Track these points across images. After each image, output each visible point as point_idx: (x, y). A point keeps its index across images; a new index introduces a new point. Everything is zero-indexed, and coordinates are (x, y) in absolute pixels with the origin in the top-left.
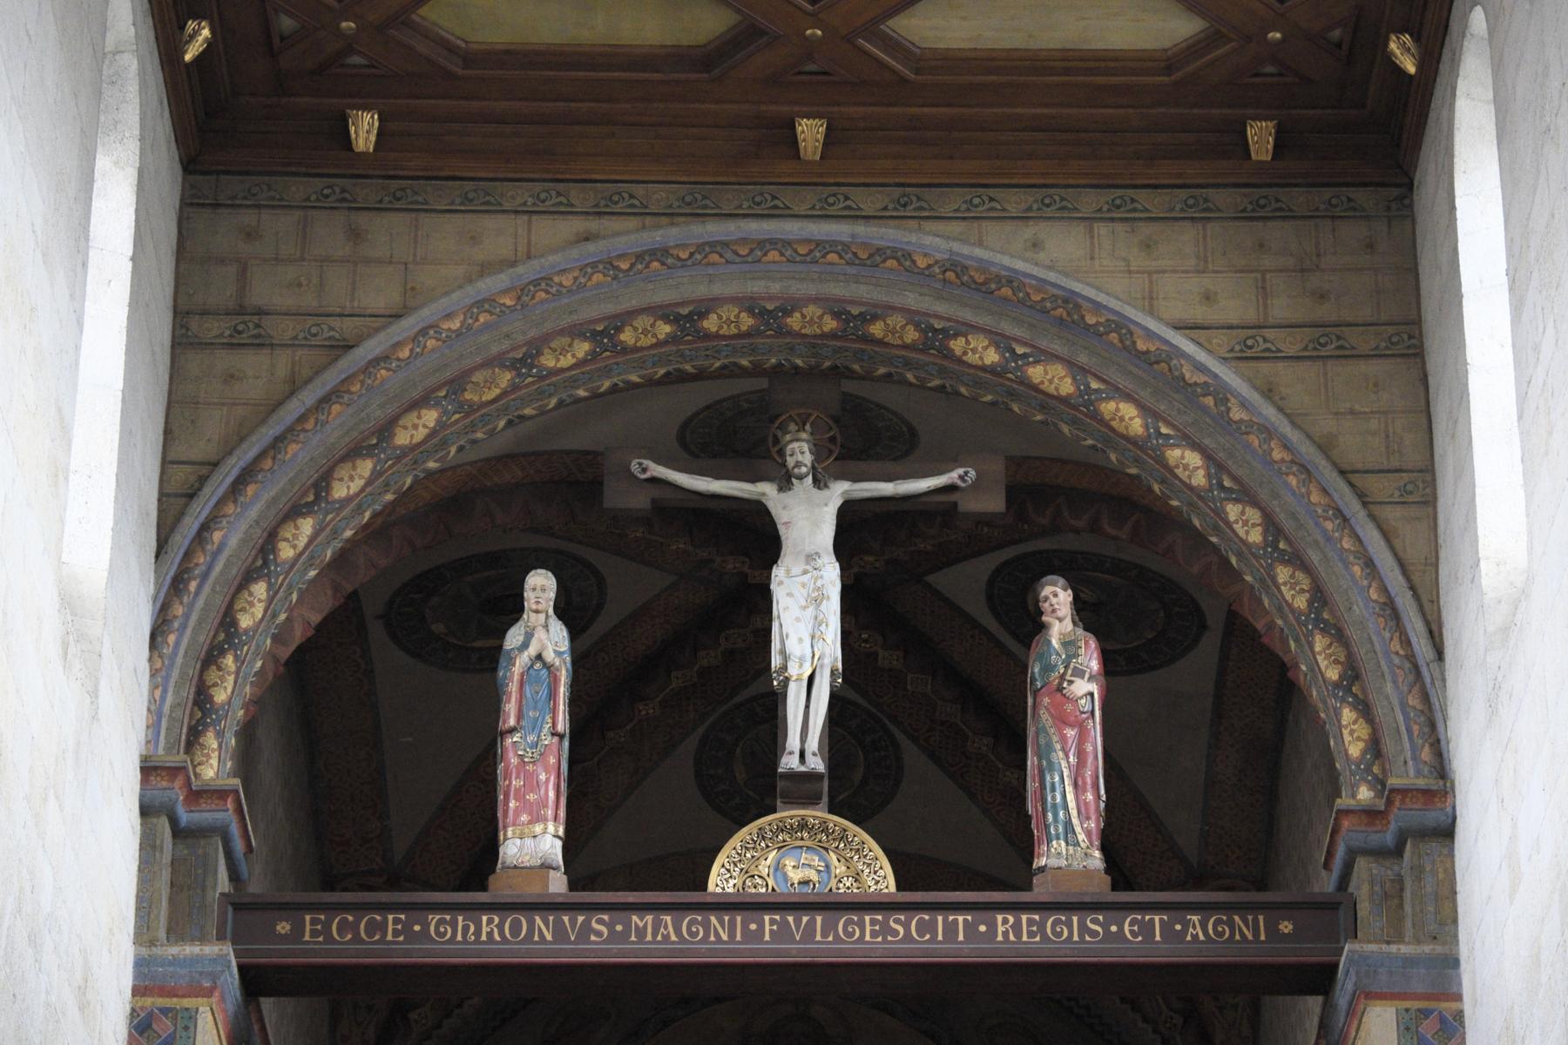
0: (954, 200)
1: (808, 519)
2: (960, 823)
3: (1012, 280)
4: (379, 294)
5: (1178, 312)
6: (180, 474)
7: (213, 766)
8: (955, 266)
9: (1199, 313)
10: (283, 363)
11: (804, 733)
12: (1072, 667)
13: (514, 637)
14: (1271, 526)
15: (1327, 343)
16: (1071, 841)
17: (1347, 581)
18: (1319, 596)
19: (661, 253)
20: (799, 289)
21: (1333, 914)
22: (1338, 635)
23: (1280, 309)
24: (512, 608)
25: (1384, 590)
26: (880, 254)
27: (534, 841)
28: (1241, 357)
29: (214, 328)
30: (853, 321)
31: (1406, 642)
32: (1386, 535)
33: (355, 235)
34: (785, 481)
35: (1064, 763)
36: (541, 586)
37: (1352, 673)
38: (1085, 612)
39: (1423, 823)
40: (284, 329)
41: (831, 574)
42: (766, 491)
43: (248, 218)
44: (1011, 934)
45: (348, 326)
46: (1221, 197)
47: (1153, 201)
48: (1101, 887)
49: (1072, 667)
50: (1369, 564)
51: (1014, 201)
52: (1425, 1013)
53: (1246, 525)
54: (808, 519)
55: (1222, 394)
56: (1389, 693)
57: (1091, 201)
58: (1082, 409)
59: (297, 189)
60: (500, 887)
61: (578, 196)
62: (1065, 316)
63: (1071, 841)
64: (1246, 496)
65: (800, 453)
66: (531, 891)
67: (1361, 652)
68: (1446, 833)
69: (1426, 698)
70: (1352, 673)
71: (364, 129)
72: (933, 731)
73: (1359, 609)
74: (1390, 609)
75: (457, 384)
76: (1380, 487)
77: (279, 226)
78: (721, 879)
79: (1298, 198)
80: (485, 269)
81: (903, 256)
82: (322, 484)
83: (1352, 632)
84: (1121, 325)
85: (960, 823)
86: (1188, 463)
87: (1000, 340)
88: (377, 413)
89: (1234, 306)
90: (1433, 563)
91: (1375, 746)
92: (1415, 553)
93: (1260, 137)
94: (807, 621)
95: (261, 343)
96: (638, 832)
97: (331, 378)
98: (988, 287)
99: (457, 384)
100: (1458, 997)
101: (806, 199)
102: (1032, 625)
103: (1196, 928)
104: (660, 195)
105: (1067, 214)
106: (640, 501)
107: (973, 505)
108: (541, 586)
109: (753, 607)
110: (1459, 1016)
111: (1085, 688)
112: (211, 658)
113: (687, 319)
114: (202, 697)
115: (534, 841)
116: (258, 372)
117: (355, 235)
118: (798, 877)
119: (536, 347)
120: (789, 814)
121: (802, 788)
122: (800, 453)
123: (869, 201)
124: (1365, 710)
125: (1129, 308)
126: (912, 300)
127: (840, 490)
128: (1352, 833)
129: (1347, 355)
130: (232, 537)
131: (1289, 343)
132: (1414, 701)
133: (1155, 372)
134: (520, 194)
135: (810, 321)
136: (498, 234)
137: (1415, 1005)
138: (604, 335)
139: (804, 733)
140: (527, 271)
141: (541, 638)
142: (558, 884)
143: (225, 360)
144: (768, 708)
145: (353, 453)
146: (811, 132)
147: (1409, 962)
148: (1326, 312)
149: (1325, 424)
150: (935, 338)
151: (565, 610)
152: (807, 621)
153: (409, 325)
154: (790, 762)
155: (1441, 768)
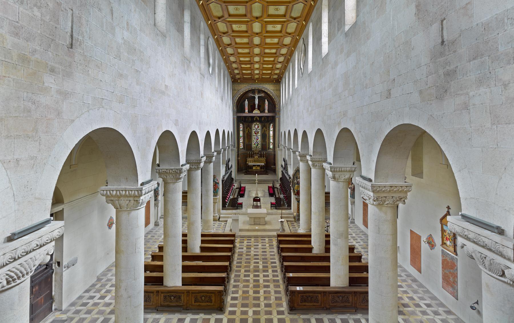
1: (257, 97)
2: (263, 111)
12: (266, 102)
15: (277, 90)
16: (266, 111)
27: (247, 111)
39: (279, 111)
44: (264, 115)
49: (266, 102)
54: (257, 97)
63: (266, 111)
72: (261, 108)
85: (263, 111)
94: (257, 102)
96: (251, 111)
115: (247, 111)
116: (236, 92)
125: (269, 88)
136: (244, 85)
144: (255, 105)
152: (257, 102)
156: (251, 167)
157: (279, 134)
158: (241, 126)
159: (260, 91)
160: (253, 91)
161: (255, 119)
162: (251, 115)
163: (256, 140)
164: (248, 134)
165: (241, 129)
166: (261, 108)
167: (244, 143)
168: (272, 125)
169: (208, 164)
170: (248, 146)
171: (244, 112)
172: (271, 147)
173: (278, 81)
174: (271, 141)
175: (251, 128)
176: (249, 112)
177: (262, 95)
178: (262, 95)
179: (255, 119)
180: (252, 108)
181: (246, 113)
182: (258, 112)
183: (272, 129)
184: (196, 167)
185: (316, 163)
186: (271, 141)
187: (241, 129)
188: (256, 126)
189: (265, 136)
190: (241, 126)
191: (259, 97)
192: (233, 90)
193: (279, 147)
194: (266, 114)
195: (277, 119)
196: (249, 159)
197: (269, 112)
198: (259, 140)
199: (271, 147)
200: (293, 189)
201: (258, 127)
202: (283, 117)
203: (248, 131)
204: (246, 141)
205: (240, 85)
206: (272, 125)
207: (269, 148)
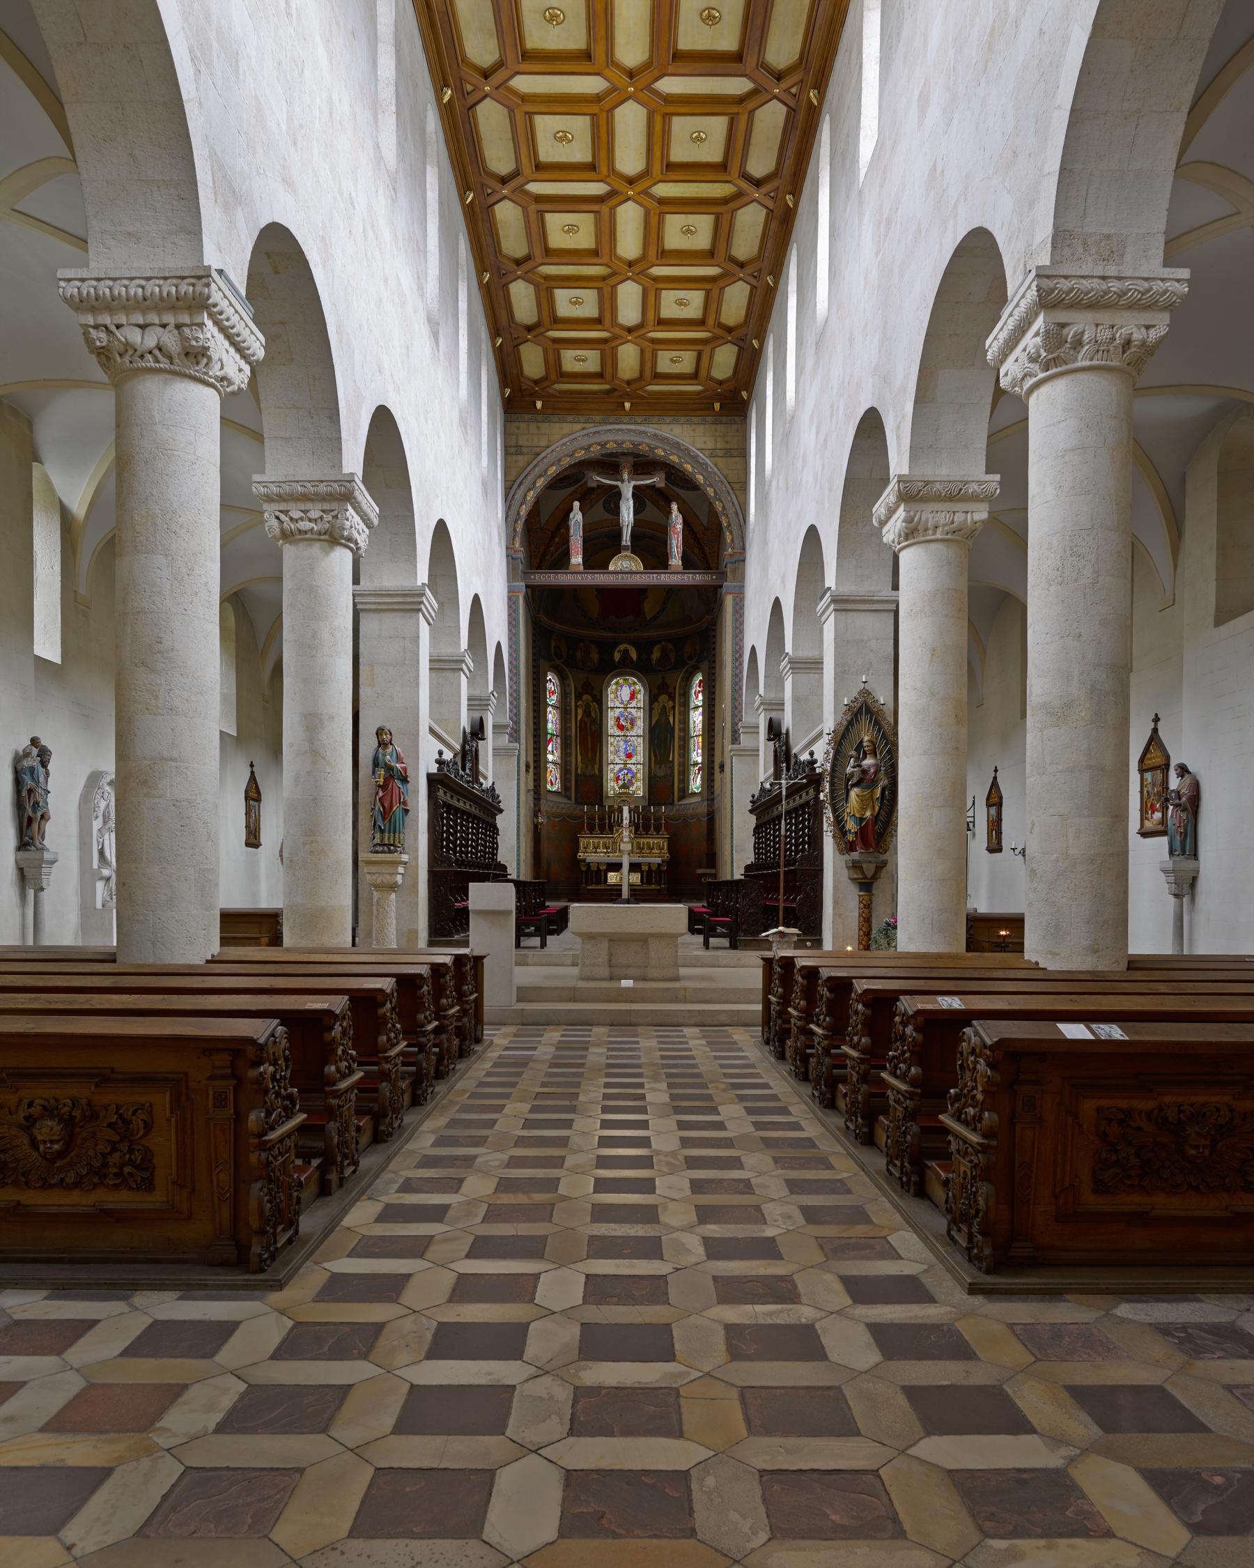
0: (655, 419)
1: (627, 490)
3: (667, 439)
4: (543, 443)
5: (698, 446)
6: (509, 484)
7: (517, 545)
8: (655, 435)
9: (703, 446)
10: (526, 458)
11: (626, 539)
13: (571, 515)
14: (715, 492)
15: (728, 453)
16: (676, 561)
17: (729, 506)
18: (724, 508)
19: (598, 432)
20: (626, 438)
21: (723, 576)
22: (727, 517)
23: (719, 446)
24: (571, 509)
26: (641, 432)
27: (577, 559)
28: (712, 456)
29: (513, 450)
30: (636, 445)
33: (538, 428)
34: (623, 481)
35: (674, 542)
36: (576, 504)
37: (729, 525)
38: (680, 510)
40: (525, 450)
41: (631, 502)
42: (619, 483)
43: (517, 424)
44: (664, 579)
45: (537, 450)
46: (709, 419)
47: (695, 419)
48: (681, 569)
51: (668, 419)
53: (710, 491)
54: (627, 490)
55: (706, 465)
56: (735, 528)
57: (683, 419)
58: (681, 464)
59: (527, 417)
60: (572, 569)
61: (582, 419)
62: (677, 446)
63: (676, 561)
64: (711, 486)
65: (626, 476)
66: (576, 570)
68: (744, 561)
70: (729, 525)
71: (539, 404)
73: (731, 512)
74: (737, 514)
75: (559, 460)
76: (736, 486)
77: (523, 425)
78: (611, 568)
79: (724, 419)
80: (564, 436)
81: (645, 433)
82: (534, 483)
84: (687, 449)
86: (700, 478)
87: (664, 450)
88: (542, 467)
89: (710, 445)
91: (732, 541)
93: (717, 406)
95: (521, 454)
97: (535, 463)
98: (664, 440)
99: (559, 460)
101: (626, 419)
102: (670, 513)
103: (698, 577)
104: (598, 418)
105: (678, 422)
106: (594, 485)
107: (658, 485)
108: (576, 504)
109: (616, 511)
111: (679, 527)
112: (516, 522)
113: (603, 445)
114: (515, 530)
115: (577, 559)
116: (522, 460)
117: (538, 428)
118: (625, 568)
119: (574, 452)
120: (623, 553)
121: (626, 548)
122: (626, 476)
123: (639, 419)
124: (731, 533)
126: (647, 441)
127: (633, 483)
128: (727, 559)
129: (731, 456)
130: (519, 496)
131: (720, 453)
133: (695, 459)
134: (570, 418)
135: (627, 445)
136: (567, 428)
138: (587, 448)
139: (626, 539)
140: (572, 437)
141: (576, 517)
142: (581, 568)
143: (515, 457)
145: (540, 476)
146: (627, 405)
148: (728, 446)
149: (726, 472)
150: (652, 449)
151: (581, 509)
153: (549, 450)
154: (624, 543)
155: (744, 549)
156: (598, 874)
157: (737, 676)
158: (552, 683)
159: (643, 465)
160: (609, 464)
161: (617, 656)
162: (598, 579)
163: (625, 760)
164: (582, 727)
165: (553, 699)
166: (650, 547)
167: (565, 766)
168: (699, 677)
169: (316, 549)
170: (585, 782)
171: (562, 561)
172: (696, 784)
173: (733, 402)
174: (697, 756)
175: (599, 700)
176: (589, 564)
177: (657, 480)
178: (657, 480)
179: (617, 656)
180: (602, 546)
181: (576, 572)
182: (635, 564)
183: (698, 699)
184: (170, 340)
185: (1082, 324)
186: (697, 756)
187: (553, 699)
188: (625, 693)
189: (664, 738)
190: (552, 683)
191: (638, 493)
192: (511, 450)
193: (735, 739)
194: (676, 574)
195: (729, 601)
196: (583, 842)
197: (688, 563)
198: (640, 757)
199: (696, 784)
201: (633, 696)
202: (765, 543)
203: (587, 713)
204: (577, 759)
205: (544, 426)
206: (699, 677)
207: (684, 792)
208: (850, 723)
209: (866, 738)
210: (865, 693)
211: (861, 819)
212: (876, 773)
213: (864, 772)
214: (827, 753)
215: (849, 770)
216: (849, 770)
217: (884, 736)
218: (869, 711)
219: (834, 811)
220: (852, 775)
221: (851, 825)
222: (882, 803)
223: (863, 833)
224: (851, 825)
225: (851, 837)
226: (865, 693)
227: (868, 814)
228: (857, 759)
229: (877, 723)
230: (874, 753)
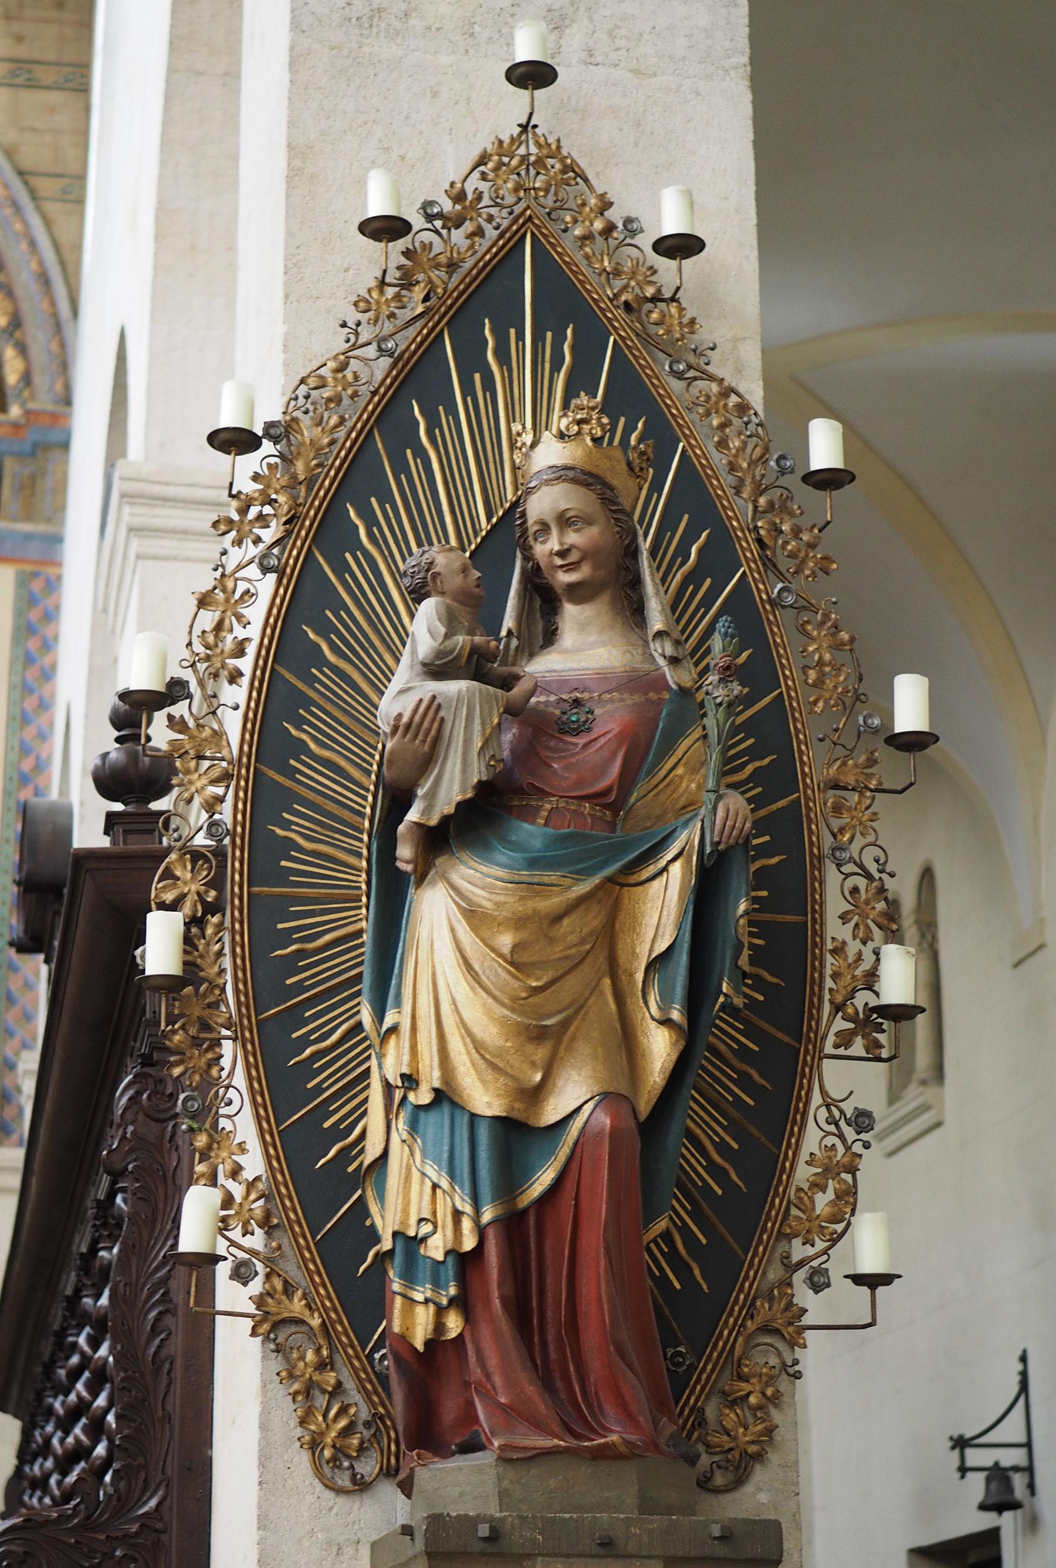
25: (41, 263)
31: (53, 304)
32: (48, 223)
50: (32, 243)
52: (35, 575)
56: (38, 338)
67: (25, 308)
69: (63, 345)
83: (19, 292)
90: (78, 246)
91: (27, 378)
92: (64, 239)
100: (59, 564)
110: (59, 578)
124: (22, 349)
132: (54, 347)
137: (29, 568)
147: (28, 537)
200: (321, 1187)
208: (415, 378)
209: (551, 453)
210: (537, 177)
211: (516, 1136)
212: (643, 749)
213: (542, 727)
214: (220, 597)
215: (401, 694)
216: (401, 694)
217: (693, 496)
218: (564, 302)
219: (282, 1089)
220: (427, 734)
221: (420, 1198)
222: (697, 999)
223: (520, 1259)
224: (420, 1198)
225: (416, 1316)
226: (537, 177)
227: (572, 1094)
228: (476, 606)
229: (630, 397)
230: (619, 587)
